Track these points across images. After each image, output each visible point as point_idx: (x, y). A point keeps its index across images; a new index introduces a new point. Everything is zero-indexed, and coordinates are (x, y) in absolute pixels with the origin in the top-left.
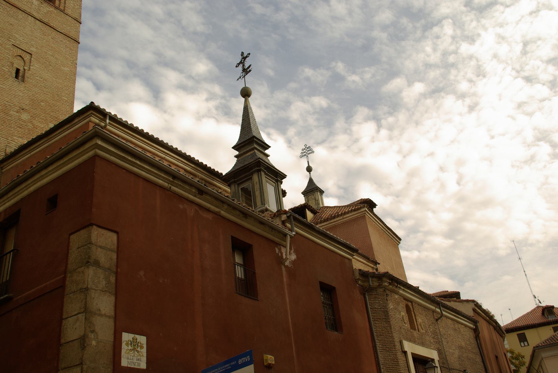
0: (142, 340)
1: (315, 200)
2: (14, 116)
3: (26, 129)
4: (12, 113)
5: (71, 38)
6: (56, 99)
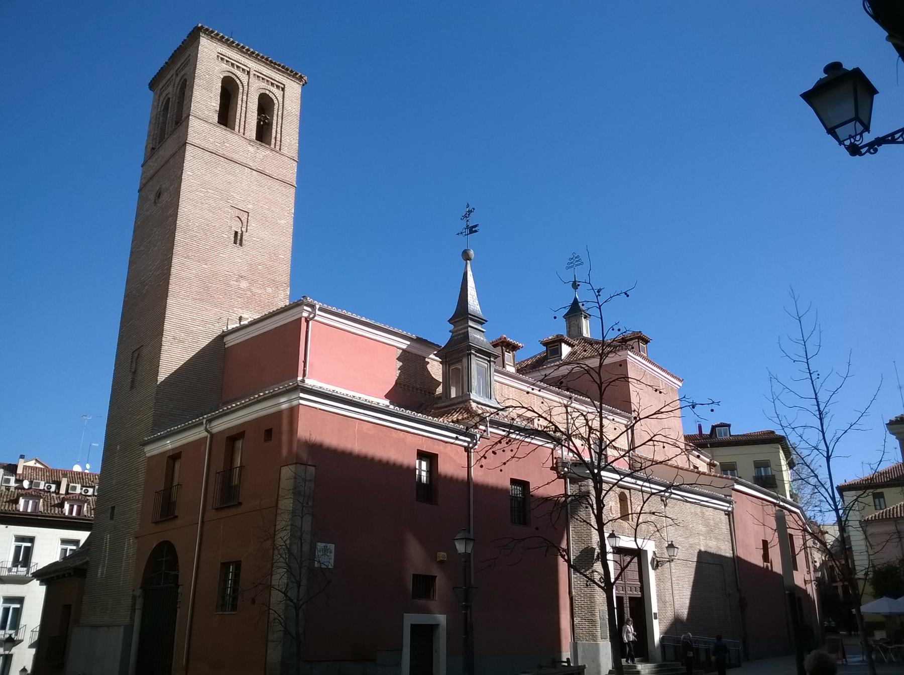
0: (332, 547)
1: (578, 327)
4: (232, 282)
5: (287, 183)
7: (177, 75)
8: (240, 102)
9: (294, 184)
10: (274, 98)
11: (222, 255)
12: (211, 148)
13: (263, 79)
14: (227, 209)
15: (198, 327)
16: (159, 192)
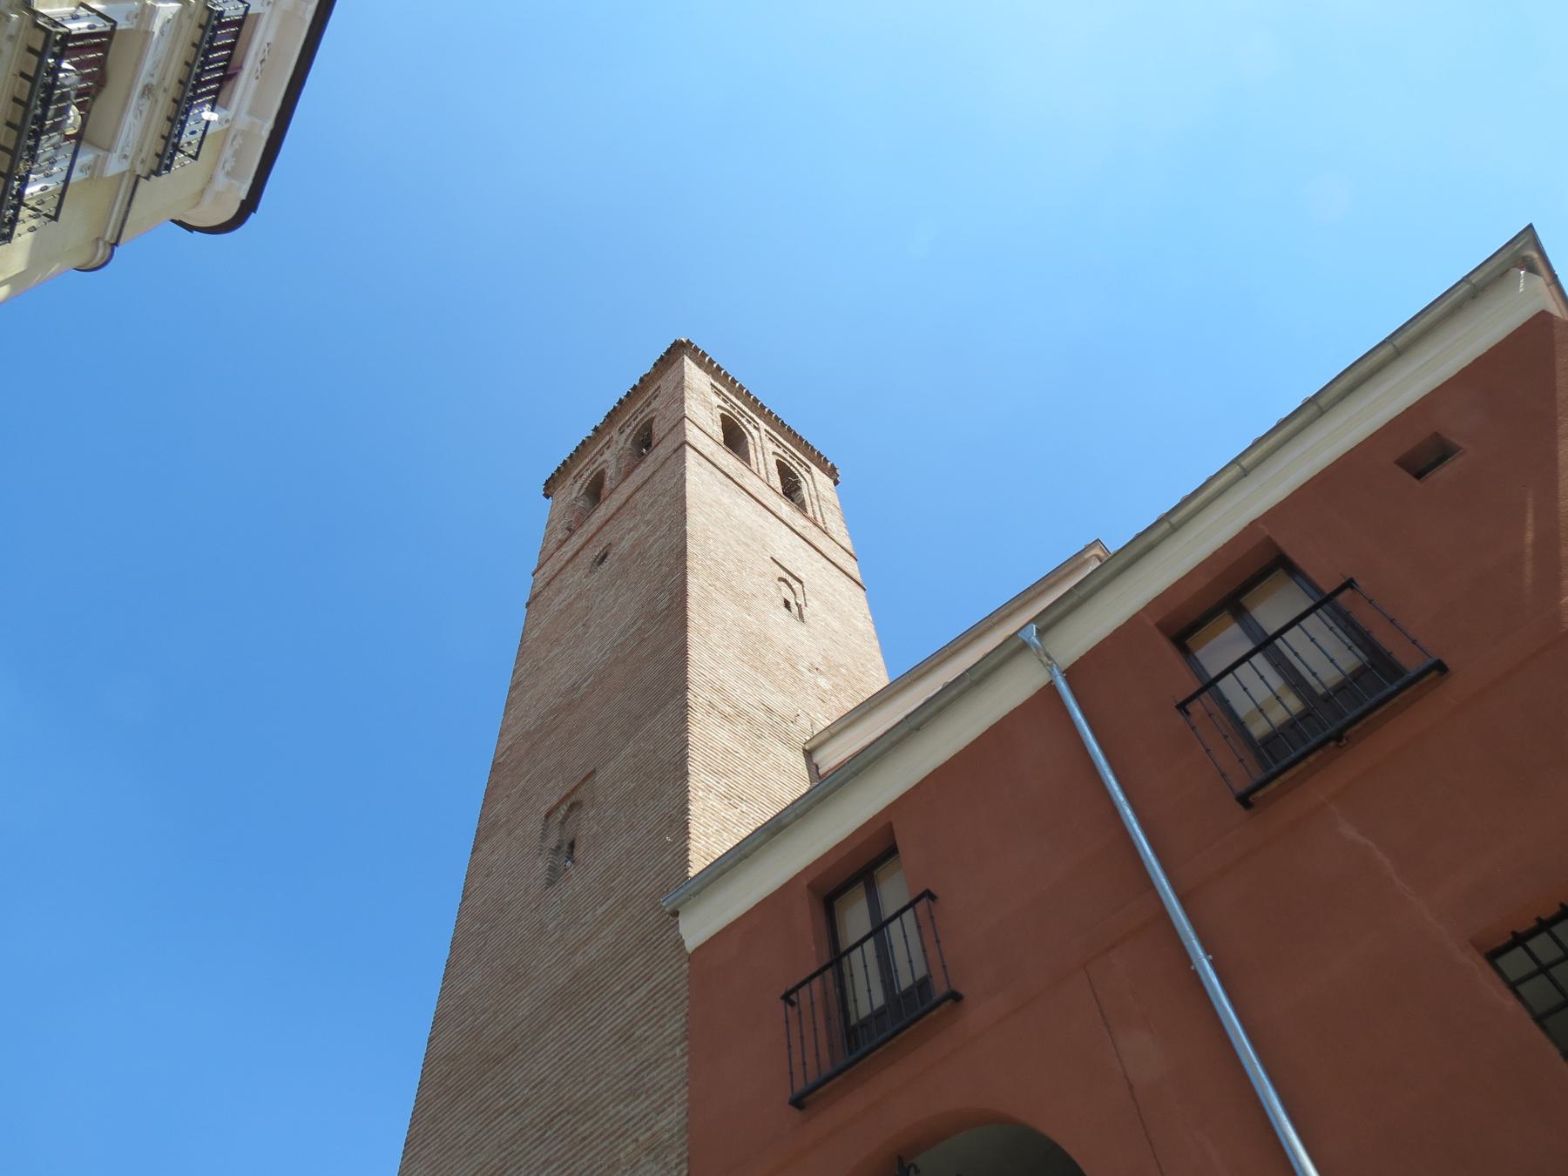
16: (605, 551)
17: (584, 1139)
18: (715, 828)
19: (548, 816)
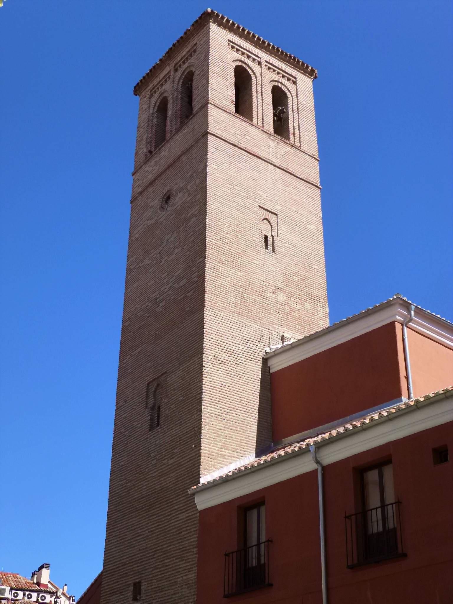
2: (271, 299)
3: (284, 314)
4: (269, 294)
6: (307, 270)
7: (176, 70)
8: (254, 93)
9: (318, 184)
10: (287, 91)
11: (255, 262)
12: (233, 140)
13: (274, 71)
14: (255, 209)
15: (239, 346)
17: (167, 566)
18: (213, 437)
19: (148, 384)
